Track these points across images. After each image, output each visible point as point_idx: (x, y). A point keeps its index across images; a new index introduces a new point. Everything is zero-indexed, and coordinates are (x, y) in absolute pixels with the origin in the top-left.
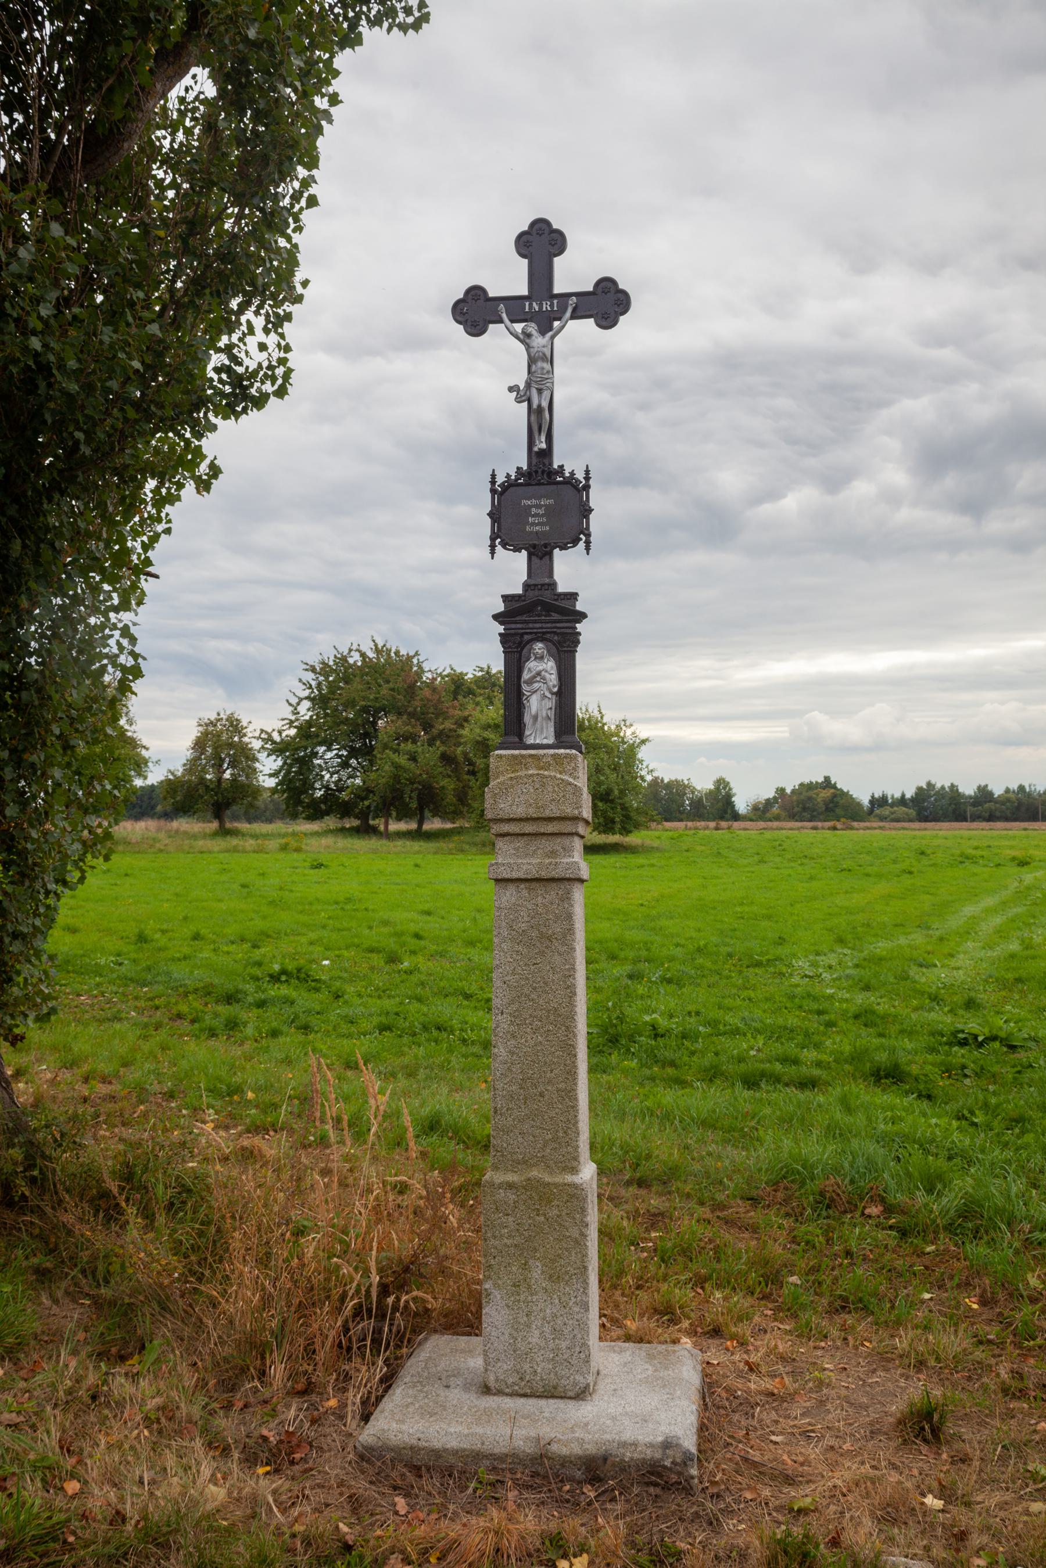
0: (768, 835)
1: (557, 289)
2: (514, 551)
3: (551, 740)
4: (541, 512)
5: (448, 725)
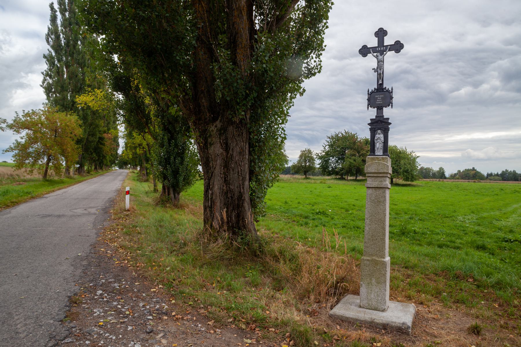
0: (454, 183)
1: (385, 45)
3: (382, 154)
5: (364, 152)
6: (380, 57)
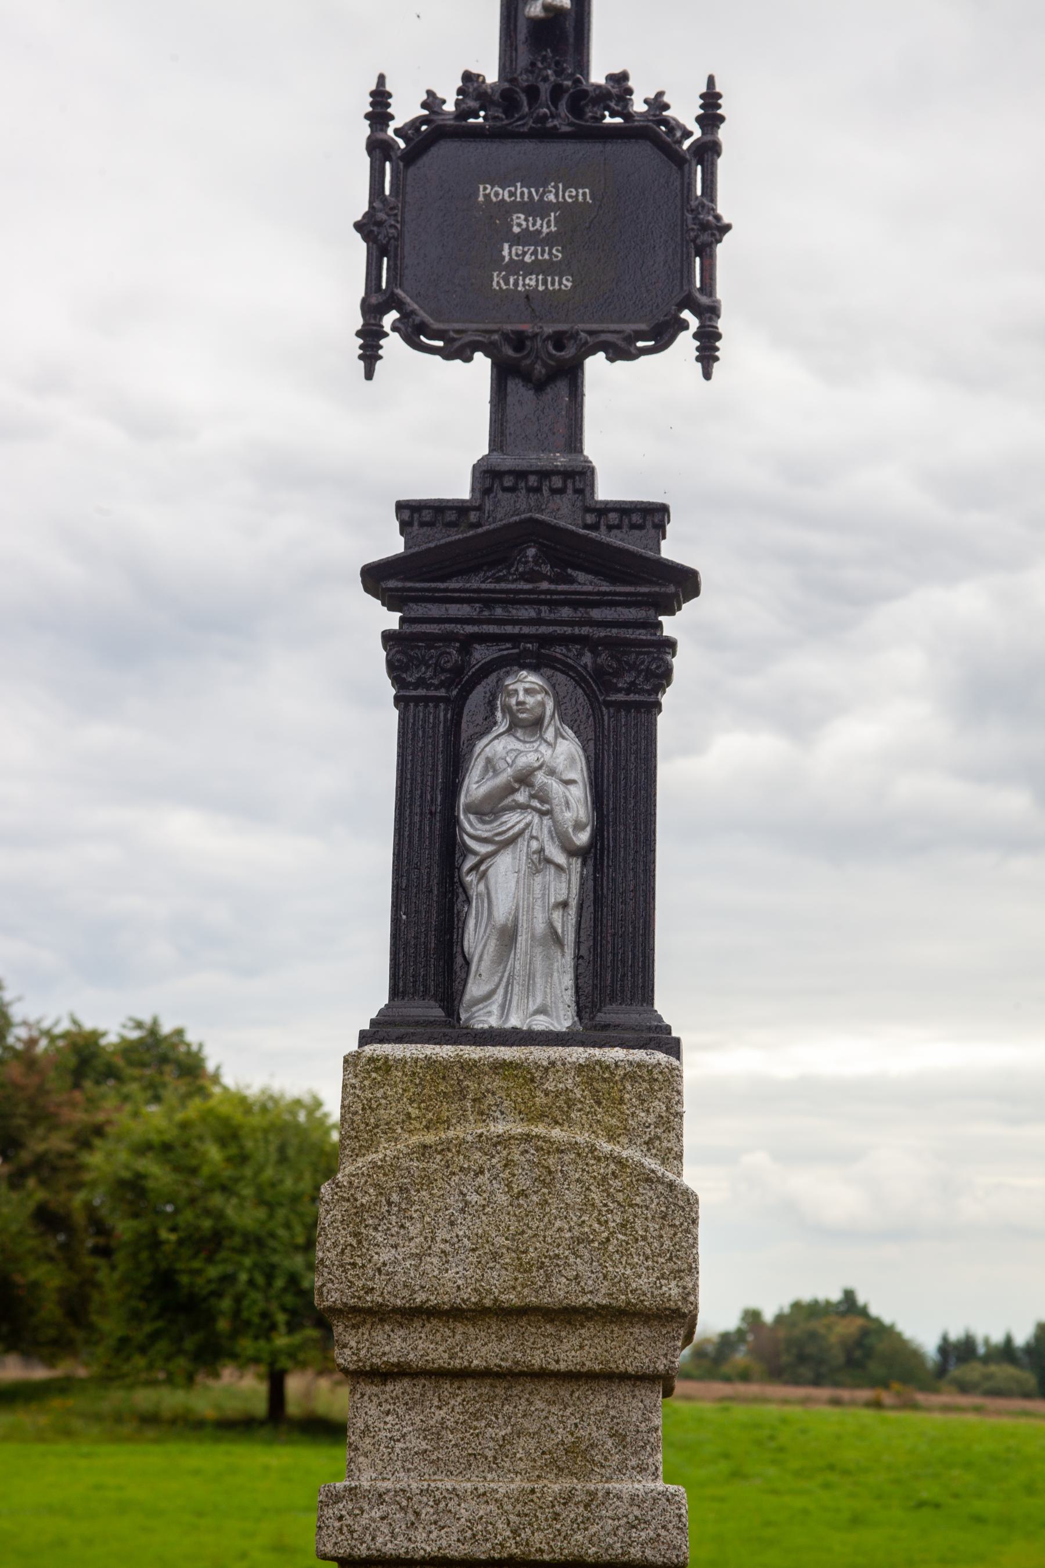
2: (448, 354)
3: (563, 1021)
4: (547, 226)
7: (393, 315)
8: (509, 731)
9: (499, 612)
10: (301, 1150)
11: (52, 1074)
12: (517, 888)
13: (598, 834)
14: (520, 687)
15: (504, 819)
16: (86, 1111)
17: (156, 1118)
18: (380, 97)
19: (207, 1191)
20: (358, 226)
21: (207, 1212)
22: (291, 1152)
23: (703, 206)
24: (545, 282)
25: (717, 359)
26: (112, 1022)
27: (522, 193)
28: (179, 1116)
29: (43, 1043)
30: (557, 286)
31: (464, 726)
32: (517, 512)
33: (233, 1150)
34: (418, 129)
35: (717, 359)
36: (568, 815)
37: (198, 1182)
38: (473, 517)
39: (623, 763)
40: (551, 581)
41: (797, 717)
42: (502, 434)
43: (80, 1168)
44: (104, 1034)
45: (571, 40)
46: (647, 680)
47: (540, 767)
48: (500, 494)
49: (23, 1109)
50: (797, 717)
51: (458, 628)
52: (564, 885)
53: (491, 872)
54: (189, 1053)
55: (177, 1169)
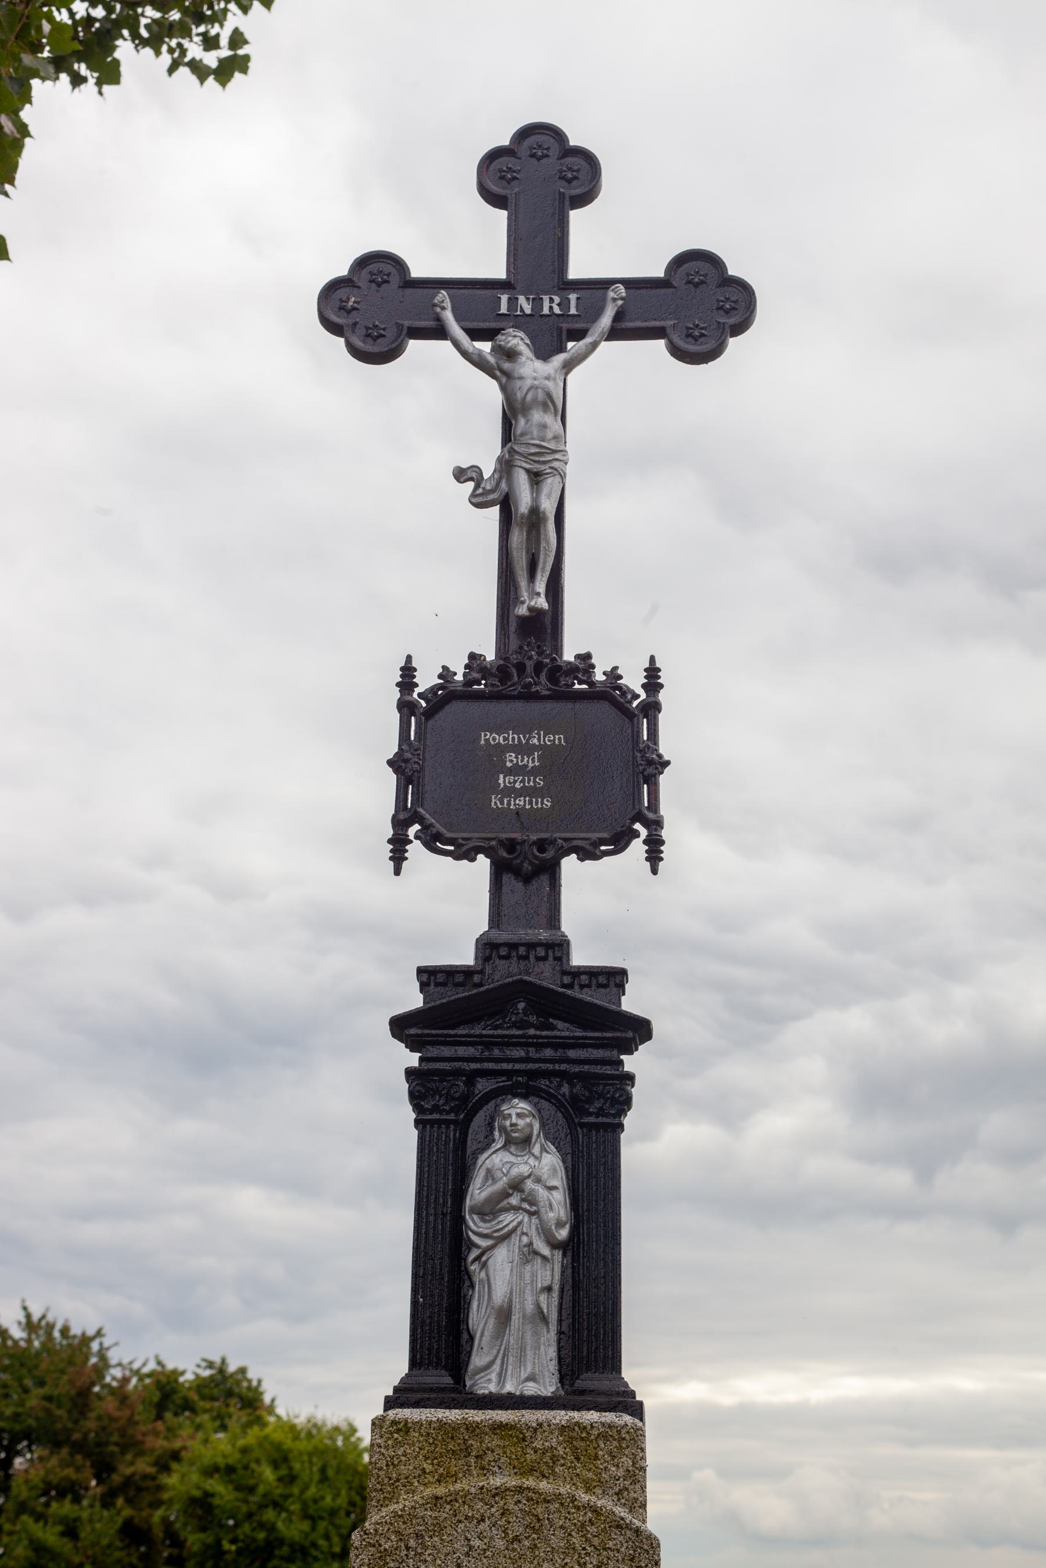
1: (575, 271)
2: (457, 856)
3: (548, 1387)
4: (532, 762)
6: (532, 369)
7: (417, 827)
8: (505, 1147)
9: (496, 1052)
10: (338, 1471)
11: (140, 1408)
12: (511, 1275)
13: (575, 1230)
14: (513, 1112)
15: (501, 1218)
16: (166, 1438)
17: (222, 1445)
18: (408, 672)
19: (262, 1507)
20: (390, 763)
21: (262, 1525)
22: (330, 1473)
23: (649, 747)
24: (531, 803)
25: (662, 859)
26: (188, 1362)
27: (513, 738)
28: (241, 1443)
29: (134, 1381)
30: (539, 806)
31: (469, 1143)
32: (510, 975)
33: (284, 1472)
34: (436, 694)
35: (662, 859)
36: (551, 1215)
37: (254, 1499)
38: (476, 978)
39: (594, 1172)
40: (537, 1029)
41: (729, 1111)
42: (499, 915)
43: (160, 1488)
44: (183, 1373)
45: (549, 631)
46: (612, 1106)
47: (529, 1176)
48: (497, 961)
49: (115, 1438)
50: (729, 1111)
51: (465, 1066)
52: (549, 1273)
53: (490, 1262)
54: (249, 1388)
55: (238, 1488)
